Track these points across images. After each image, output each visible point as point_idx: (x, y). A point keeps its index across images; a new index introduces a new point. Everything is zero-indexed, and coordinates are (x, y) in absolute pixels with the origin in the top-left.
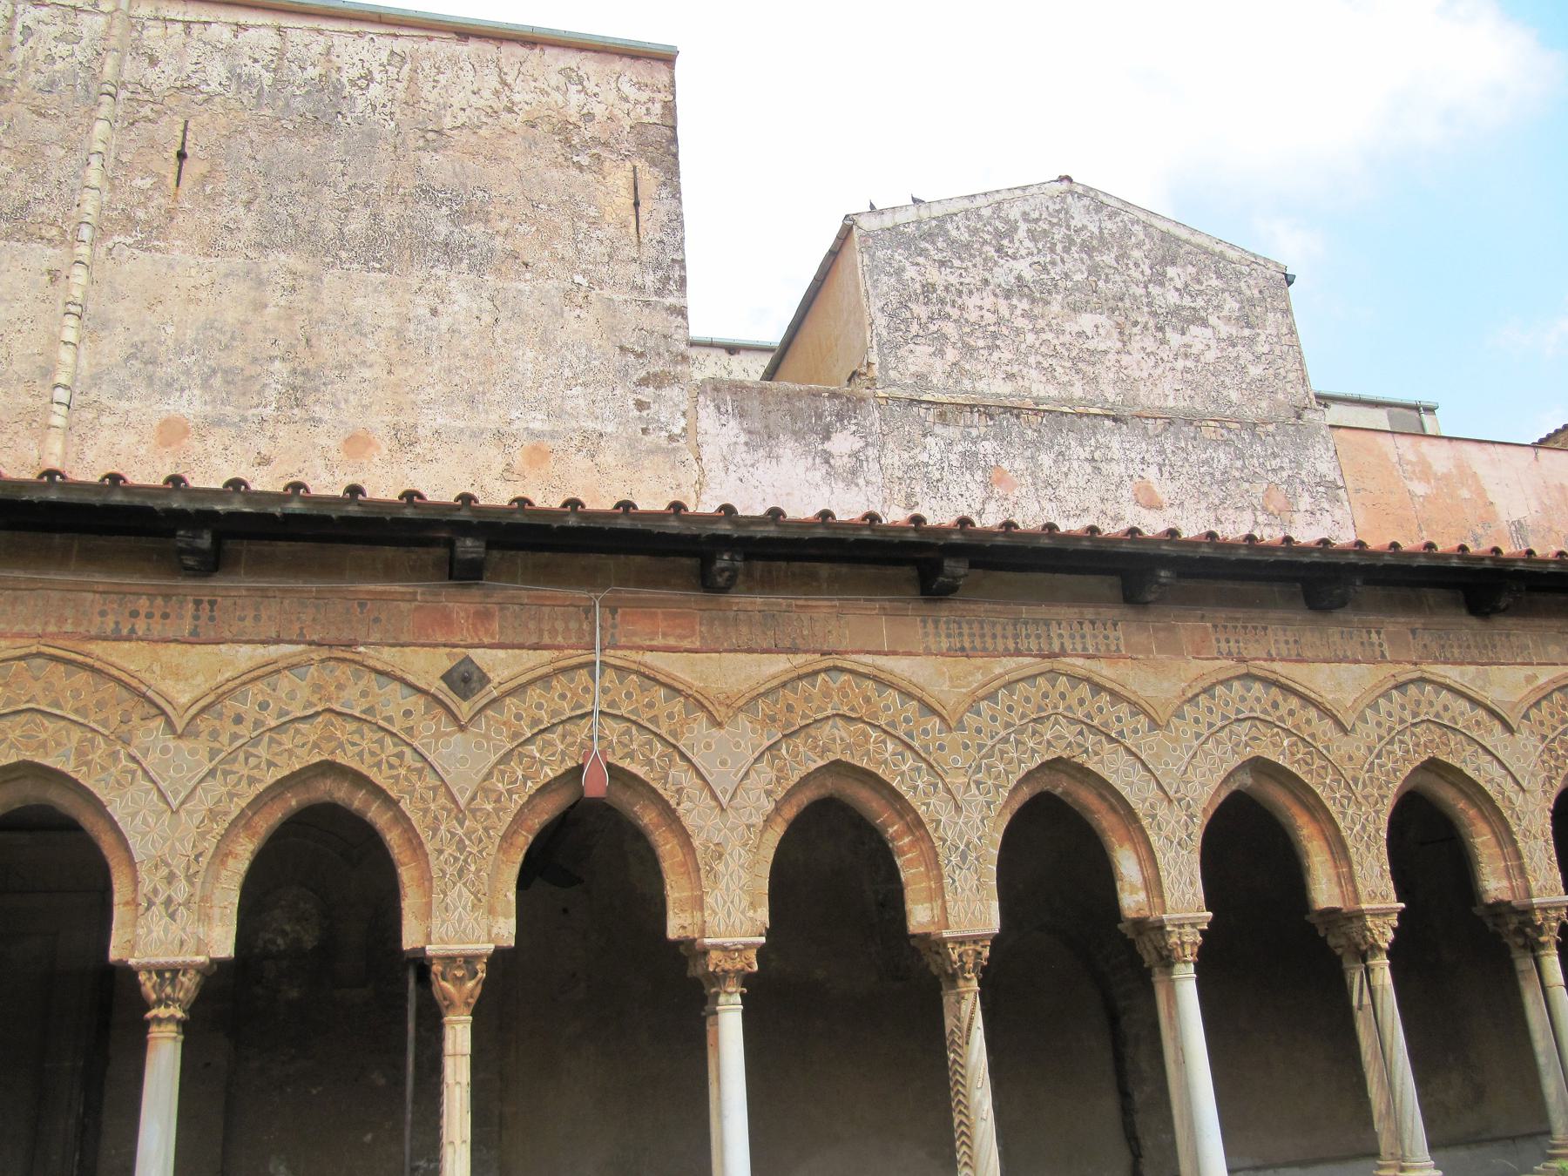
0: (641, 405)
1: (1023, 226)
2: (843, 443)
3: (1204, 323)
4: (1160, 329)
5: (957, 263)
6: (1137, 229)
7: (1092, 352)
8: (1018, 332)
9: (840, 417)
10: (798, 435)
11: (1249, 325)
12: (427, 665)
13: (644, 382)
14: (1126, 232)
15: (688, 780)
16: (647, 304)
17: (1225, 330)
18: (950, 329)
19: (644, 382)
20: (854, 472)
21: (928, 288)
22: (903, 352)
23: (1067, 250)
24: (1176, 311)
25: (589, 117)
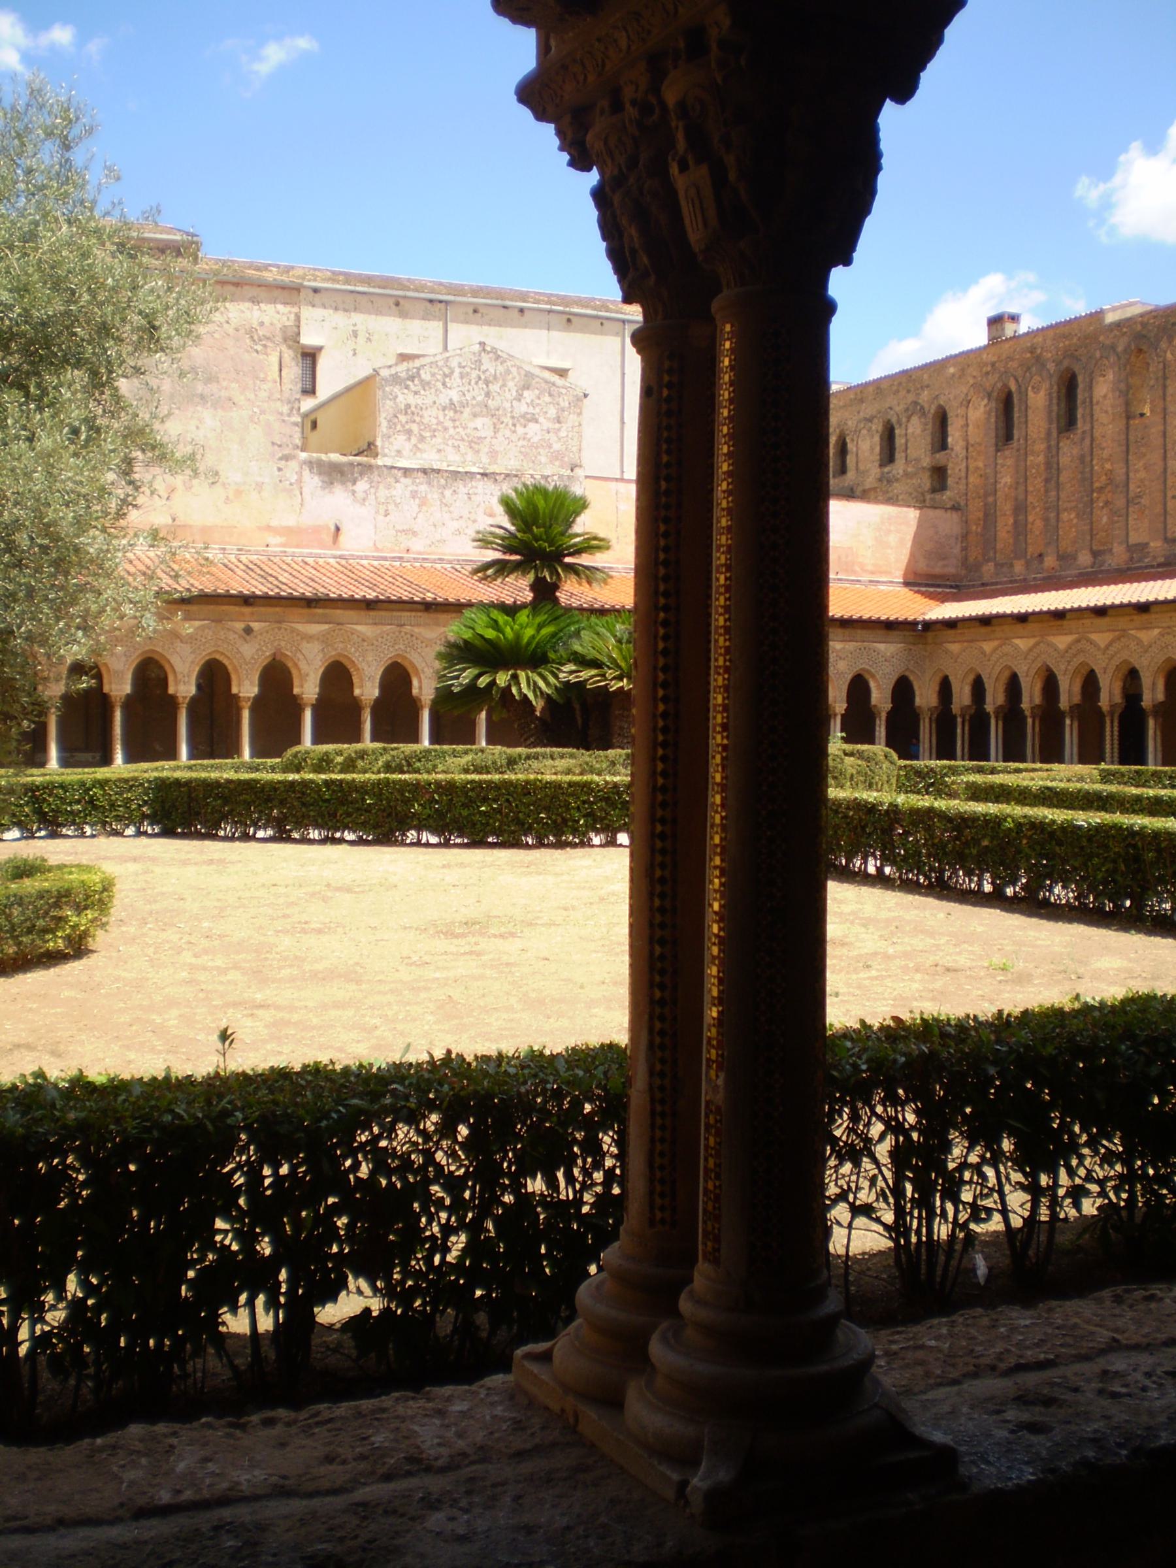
0: (280, 469)
1: (457, 370)
2: (362, 485)
3: (537, 421)
4: (514, 425)
5: (422, 392)
6: (514, 370)
7: (479, 438)
8: (446, 429)
9: (361, 474)
10: (343, 483)
11: (559, 422)
12: (240, 626)
13: (281, 459)
14: (508, 372)
15: (301, 657)
16: (284, 421)
17: (547, 424)
18: (415, 427)
19: (281, 459)
20: (364, 500)
21: (408, 406)
22: (392, 440)
23: (477, 383)
24: (523, 416)
25: (262, 324)
